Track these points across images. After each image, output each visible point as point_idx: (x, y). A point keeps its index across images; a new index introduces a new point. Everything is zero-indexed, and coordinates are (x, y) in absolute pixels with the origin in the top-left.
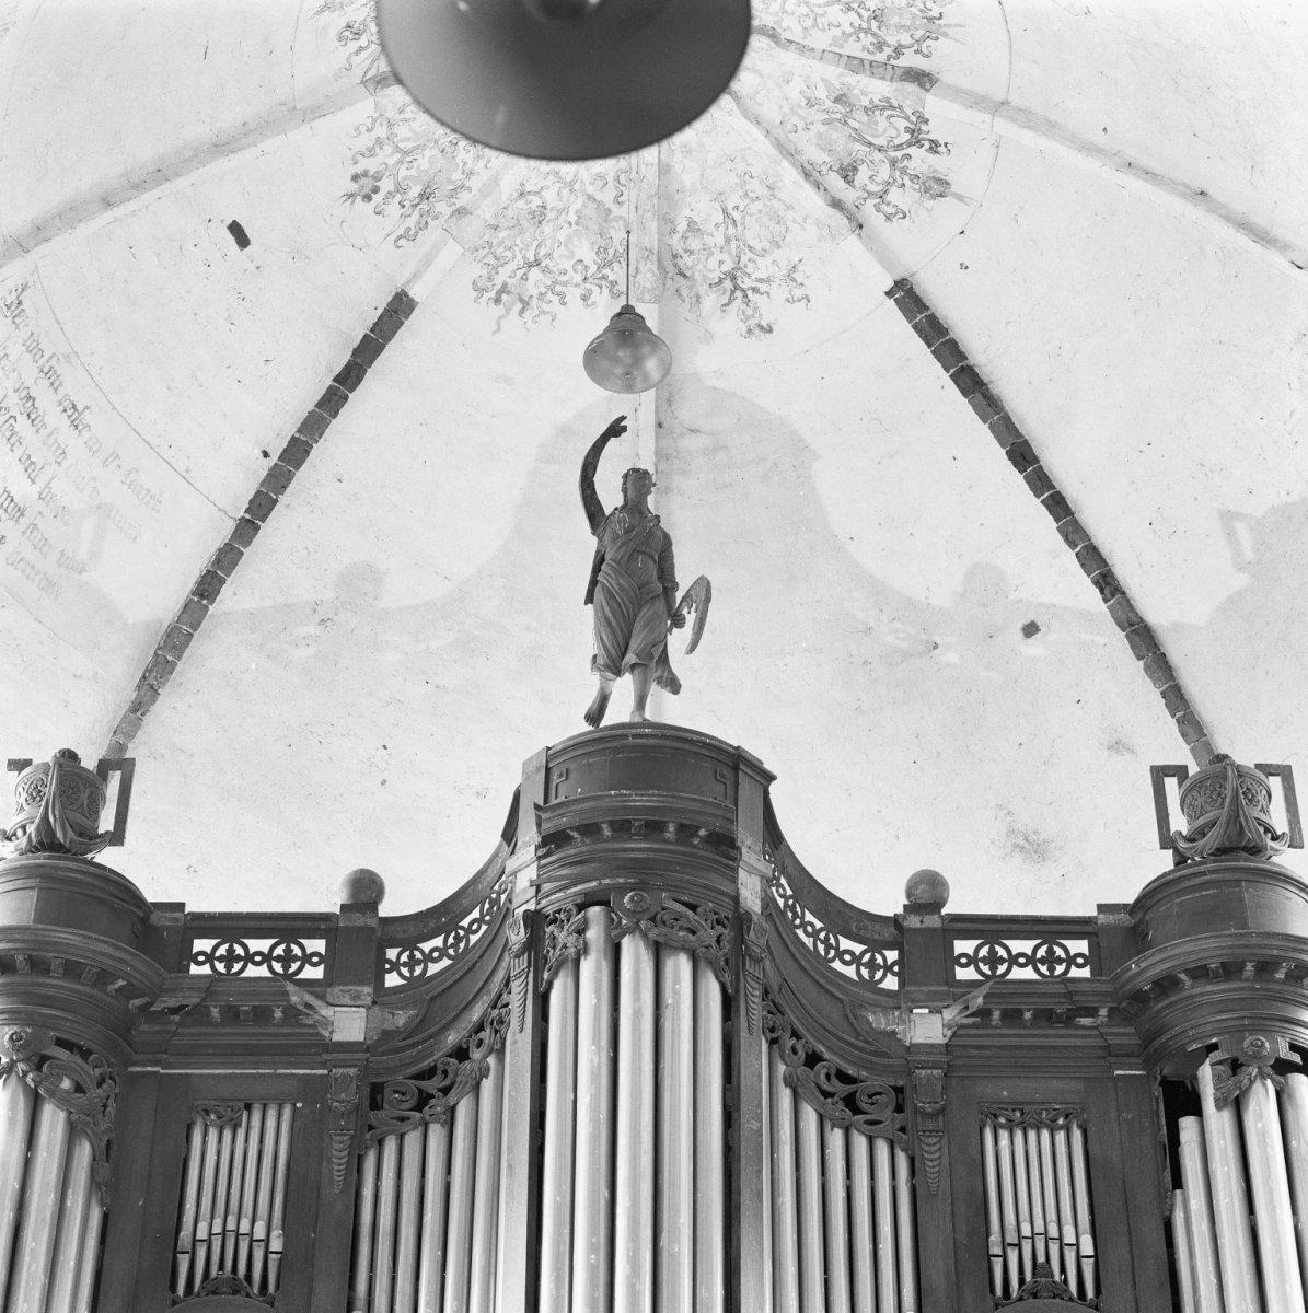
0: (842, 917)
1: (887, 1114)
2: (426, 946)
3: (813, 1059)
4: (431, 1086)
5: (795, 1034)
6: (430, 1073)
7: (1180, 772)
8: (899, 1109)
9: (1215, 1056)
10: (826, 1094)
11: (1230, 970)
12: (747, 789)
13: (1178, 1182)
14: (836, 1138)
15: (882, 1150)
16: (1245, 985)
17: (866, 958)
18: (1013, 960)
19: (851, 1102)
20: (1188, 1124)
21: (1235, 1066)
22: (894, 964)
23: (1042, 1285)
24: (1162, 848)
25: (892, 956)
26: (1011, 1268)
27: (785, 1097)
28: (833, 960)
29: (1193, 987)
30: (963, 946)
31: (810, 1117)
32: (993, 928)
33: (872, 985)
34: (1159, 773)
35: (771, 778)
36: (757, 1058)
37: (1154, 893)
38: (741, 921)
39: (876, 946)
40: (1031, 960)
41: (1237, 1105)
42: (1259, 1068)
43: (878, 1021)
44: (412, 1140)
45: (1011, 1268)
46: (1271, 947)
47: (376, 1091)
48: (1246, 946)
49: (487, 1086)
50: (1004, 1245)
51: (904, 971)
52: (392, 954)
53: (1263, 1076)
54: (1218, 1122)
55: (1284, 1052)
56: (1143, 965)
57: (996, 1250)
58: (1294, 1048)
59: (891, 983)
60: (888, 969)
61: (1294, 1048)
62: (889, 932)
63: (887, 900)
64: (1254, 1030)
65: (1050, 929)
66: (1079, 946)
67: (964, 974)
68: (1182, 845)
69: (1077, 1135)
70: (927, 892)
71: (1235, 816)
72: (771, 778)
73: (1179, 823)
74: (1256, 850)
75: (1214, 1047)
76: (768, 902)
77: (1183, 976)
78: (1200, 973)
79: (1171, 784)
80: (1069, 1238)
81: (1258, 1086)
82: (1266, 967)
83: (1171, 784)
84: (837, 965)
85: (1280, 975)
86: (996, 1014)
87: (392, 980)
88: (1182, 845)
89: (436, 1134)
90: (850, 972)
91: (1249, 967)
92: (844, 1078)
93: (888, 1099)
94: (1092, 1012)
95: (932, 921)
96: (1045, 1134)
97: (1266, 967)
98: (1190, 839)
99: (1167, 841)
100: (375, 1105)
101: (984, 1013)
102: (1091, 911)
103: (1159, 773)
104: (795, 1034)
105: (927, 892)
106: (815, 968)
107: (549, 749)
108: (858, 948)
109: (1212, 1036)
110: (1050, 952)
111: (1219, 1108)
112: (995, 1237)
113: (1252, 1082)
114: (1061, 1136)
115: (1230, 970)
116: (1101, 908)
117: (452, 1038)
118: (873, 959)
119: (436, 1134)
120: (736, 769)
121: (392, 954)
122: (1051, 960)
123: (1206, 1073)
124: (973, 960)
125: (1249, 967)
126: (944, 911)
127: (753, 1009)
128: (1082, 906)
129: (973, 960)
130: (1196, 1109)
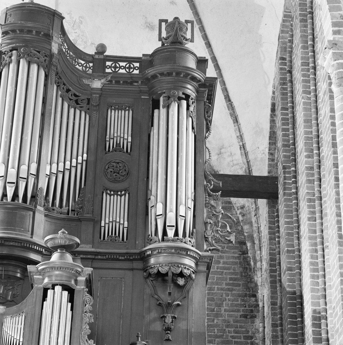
0: (80, 54)
1: (84, 105)
5: (64, 84)
7: (166, 21)
8: (88, 104)
9: (164, 95)
10: (71, 100)
11: (169, 74)
12: (57, 21)
13: (152, 125)
14: (72, 110)
16: (173, 78)
17: (85, 65)
18: (120, 67)
19: (77, 102)
20: (156, 111)
21: (169, 98)
22: (91, 67)
23: (118, 148)
24: (159, 41)
25: (91, 65)
26: (111, 144)
27: (60, 100)
28: (76, 65)
29: (160, 77)
30: (108, 63)
32: (116, 59)
33: (85, 72)
34: (161, 21)
35: (63, 18)
37: (156, 52)
38: (51, 56)
39: (87, 62)
40: (125, 68)
41: (168, 107)
42: (174, 98)
43: (86, 81)
45: (111, 144)
46: (179, 69)
48: (173, 68)
50: (110, 138)
51: (94, 69)
53: (175, 101)
54: (163, 111)
55: (181, 95)
56: (149, 72)
57: (108, 140)
58: (183, 94)
60: (90, 68)
61: (183, 94)
62: (91, 59)
63: (91, 51)
64: (174, 89)
65: (130, 60)
66: (137, 65)
67: (108, 71)
68: (164, 41)
69: (131, 112)
70: (101, 49)
71: (176, 35)
72: (63, 18)
73: (164, 34)
74: (181, 43)
75: (164, 93)
76: (60, 51)
77: (158, 75)
78: (162, 74)
79: (163, 24)
80: (126, 137)
81: (173, 103)
82: (178, 74)
83: (163, 24)
84: (77, 66)
85: (182, 76)
86: (114, 82)
88: (164, 41)
90: (80, 68)
91: (174, 73)
92: (75, 95)
93: (86, 101)
94: (137, 82)
95: (101, 57)
96: (123, 112)
97: (178, 74)
98: (166, 39)
99: (160, 39)
101: (110, 81)
102: (141, 56)
103: (161, 21)
104: (64, 84)
105: (101, 49)
107: (7, 8)
108: (83, 62)
109: (164, 90)
110: (130, 66)
111: (163, 108)
112: (108, 136)
113: (172, 102)
114: (127, 112)
115: (169, 74)
116: (144, 55)
118: (86, 65)
120: (54, 16)
122: (130, 68)
123: (161, 99)
124: (110, 67)
125: (174, 73)
126: (105, 54)
127: (53, 77)
128: (138, 54)
129: (110, 67)
130: (159, 108)
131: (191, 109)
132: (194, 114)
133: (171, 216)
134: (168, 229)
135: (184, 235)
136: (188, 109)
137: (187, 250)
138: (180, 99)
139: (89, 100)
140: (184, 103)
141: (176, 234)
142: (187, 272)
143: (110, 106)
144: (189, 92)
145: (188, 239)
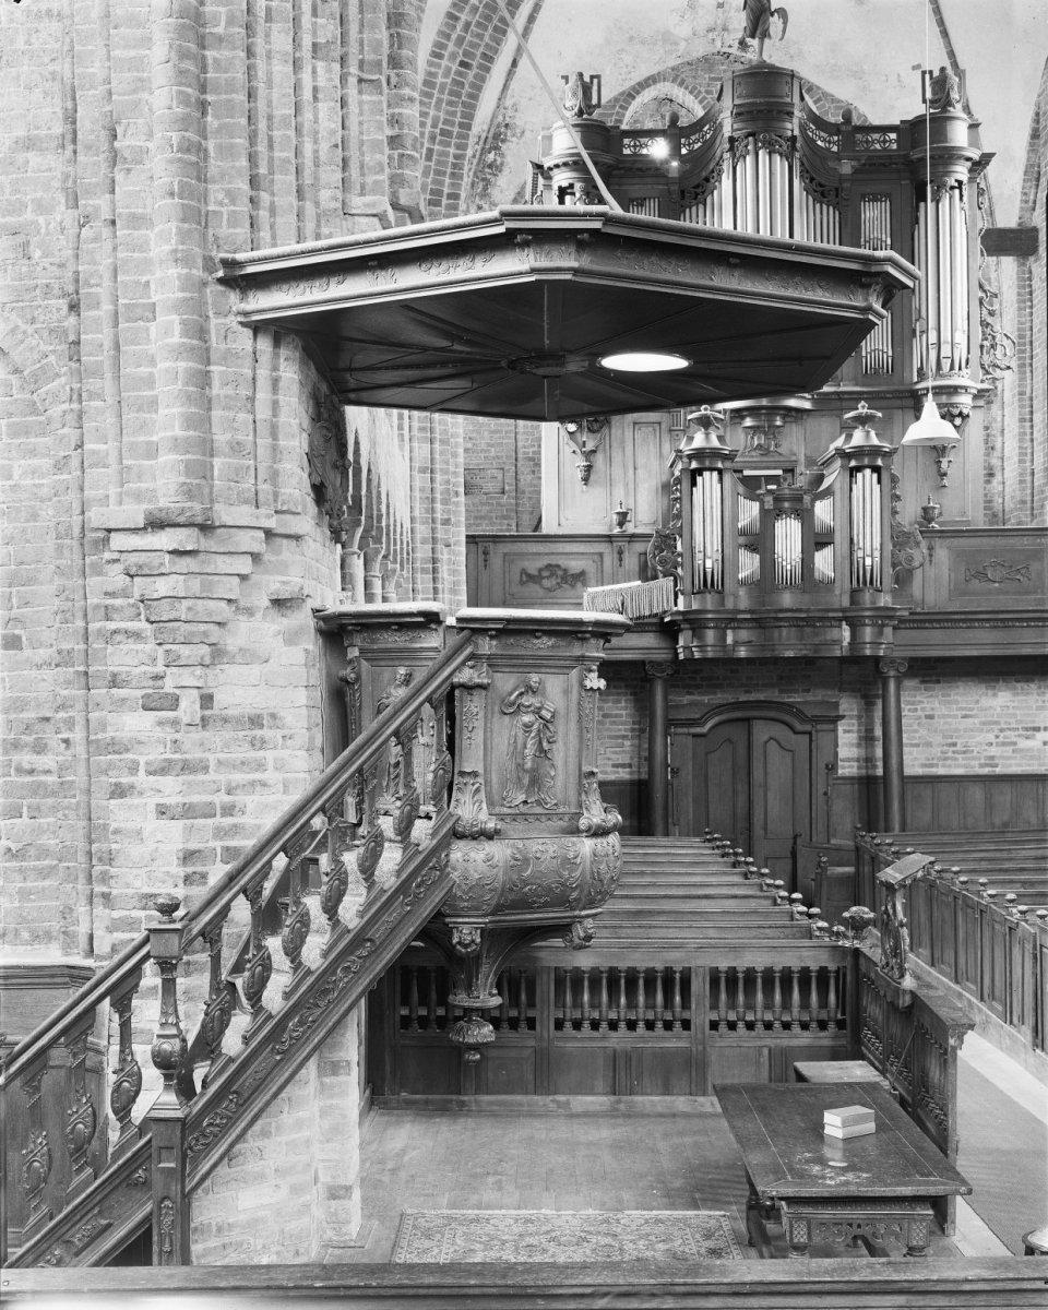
2: (693, 138)
3: (812, 180)
4: (699, 190)
6: (697, 186)
13: (917, 223)
14: (818, 206)
15: (831, 208)
19: (823, 195)
20: (922, 204)
31: (810, 198)
33: (828, 149)
34: (924, 73)
36: (796, 182)
41: (937, 201)
43: (831, 164)
44: (694, 209)
47: (683, 192)
49: (715, 192)
52: (683, 140)
54: (930, 205)
59: (835, 149)
66: (893, 136)
73: (929, 95)
83: (927, 76)
84: (819, 143)
87: (684, 151)
89: (701, 206)
92: (821, 185)
99: (924, 101)
100: (683, 197)
106: (810, 142)
108: (825, 135)
117: (704, 174)
119: (701, 206)
121: (683, 140)
122: (885, 141)
130: (925, 201)
131: (965, 199)
132: (966, 207)
133: (945, 351)
134: (943, 361)
135: (960, 369)
136: (961, 199)
137: (966, 388)
138: (952, 188)
139: (837, 189)
140: (957, 191)
141: (952, 368)
142: (965, 411)
143: (863, 197)
144: (960, 177)
145: (964, 370)
